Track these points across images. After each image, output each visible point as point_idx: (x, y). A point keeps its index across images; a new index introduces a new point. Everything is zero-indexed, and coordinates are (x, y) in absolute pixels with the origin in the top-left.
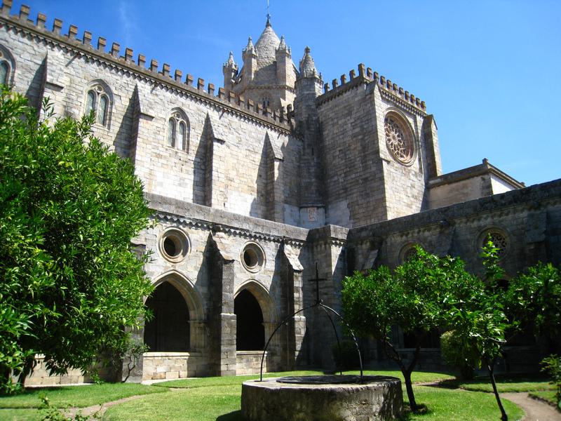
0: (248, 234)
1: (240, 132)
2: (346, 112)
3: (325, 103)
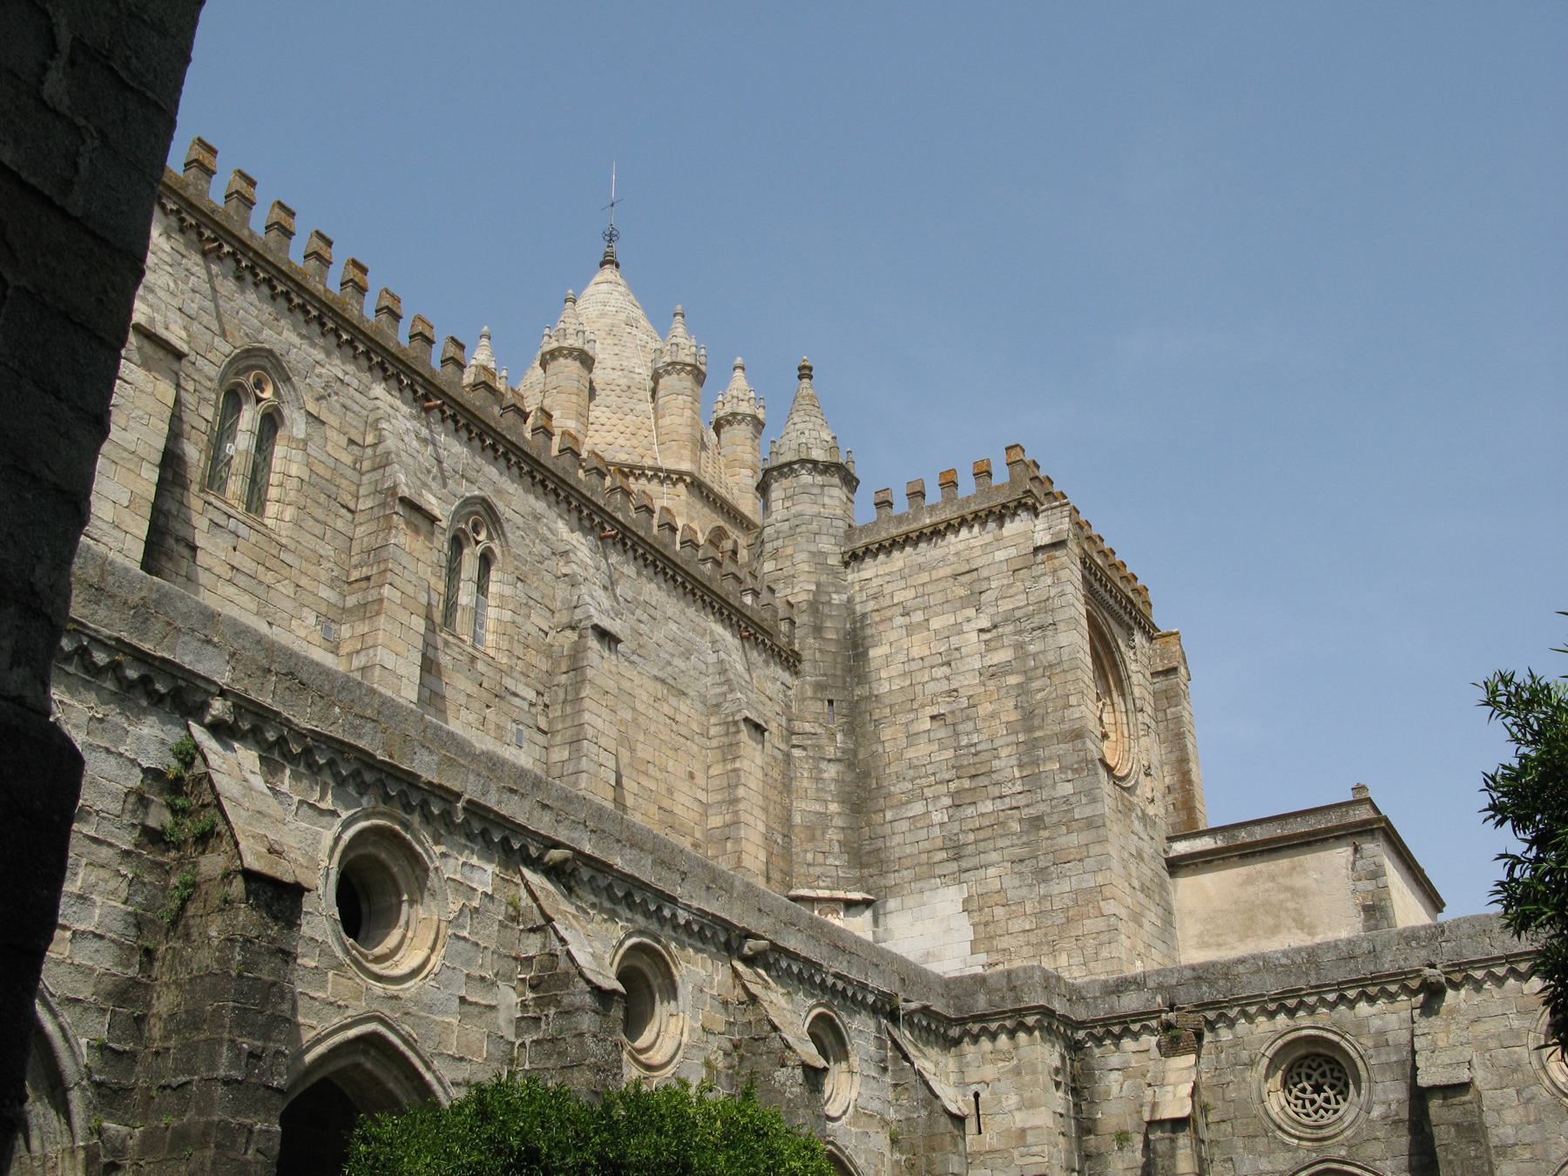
2: (962, 592)
3: (876, 556)
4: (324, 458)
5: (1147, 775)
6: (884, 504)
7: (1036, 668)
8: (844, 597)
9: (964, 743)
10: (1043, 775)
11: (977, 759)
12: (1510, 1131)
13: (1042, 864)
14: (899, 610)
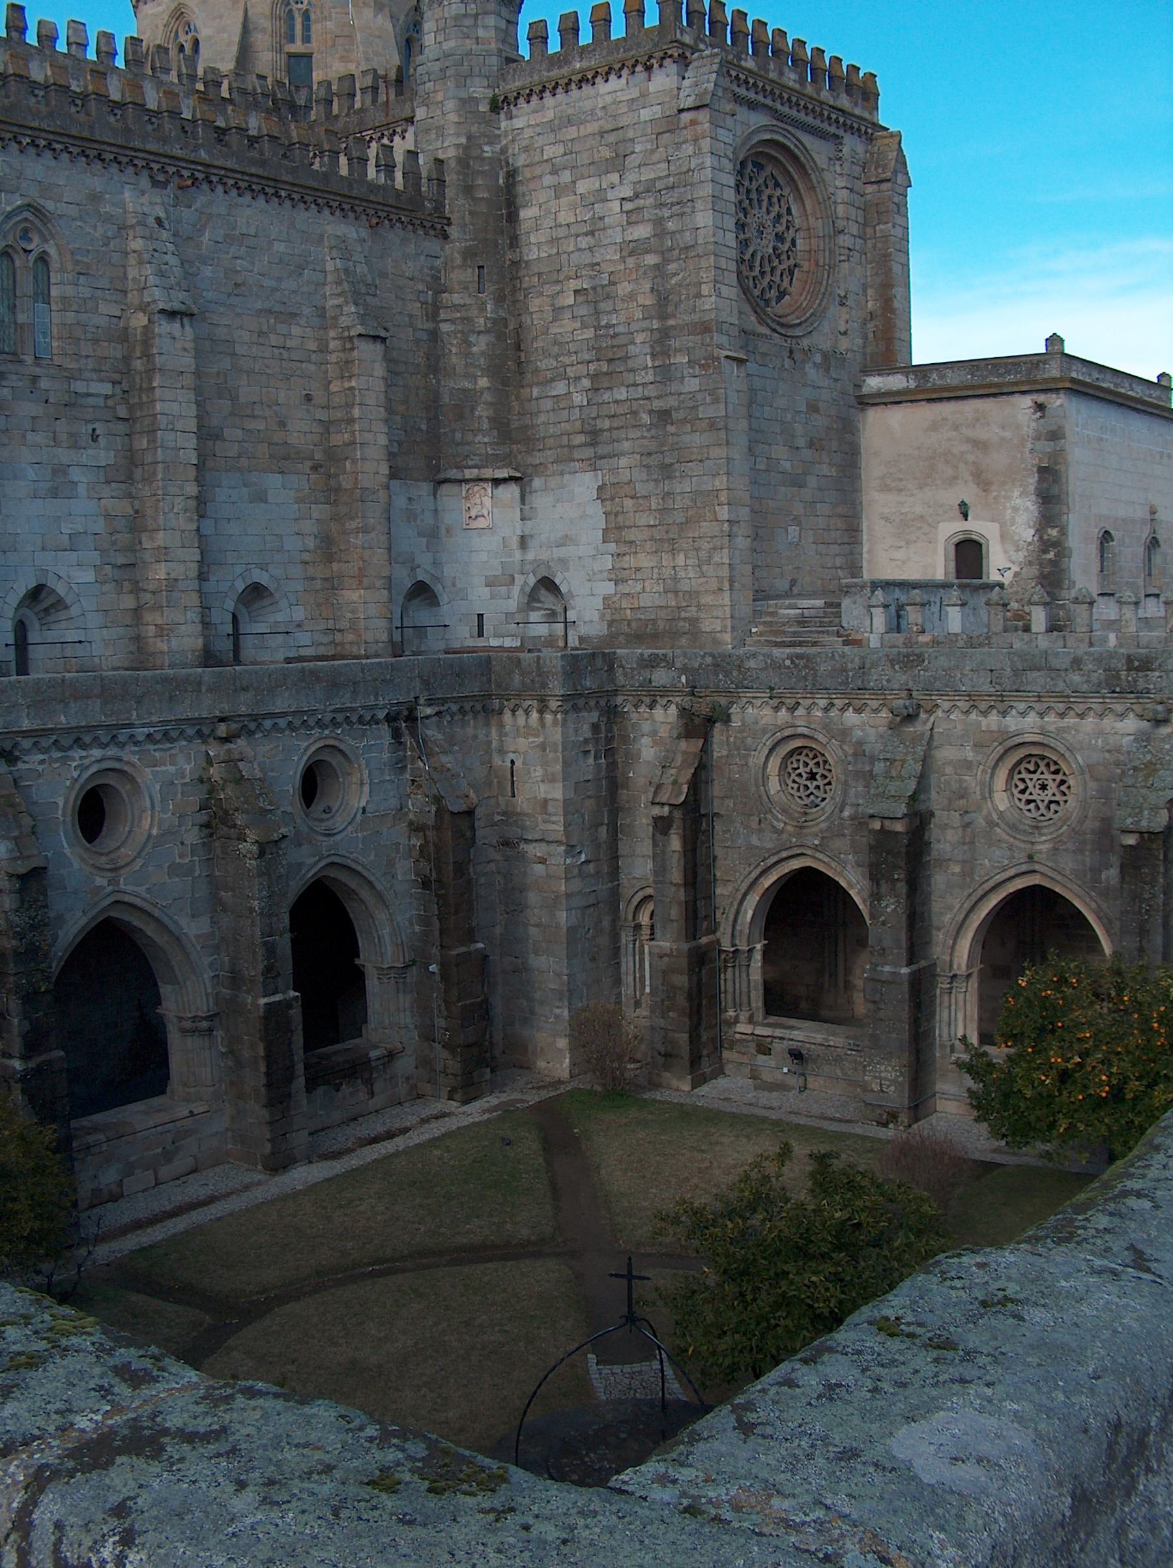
2: (606, 153)
5: (842, 304)
6: (538, 36)
7: (672, 249)
8: (498, 148)
9: (603, 323)
10: (673, 368)
11: (615, 342)
12: (948, 848)
13: (668, 461)
14: (548, 167)
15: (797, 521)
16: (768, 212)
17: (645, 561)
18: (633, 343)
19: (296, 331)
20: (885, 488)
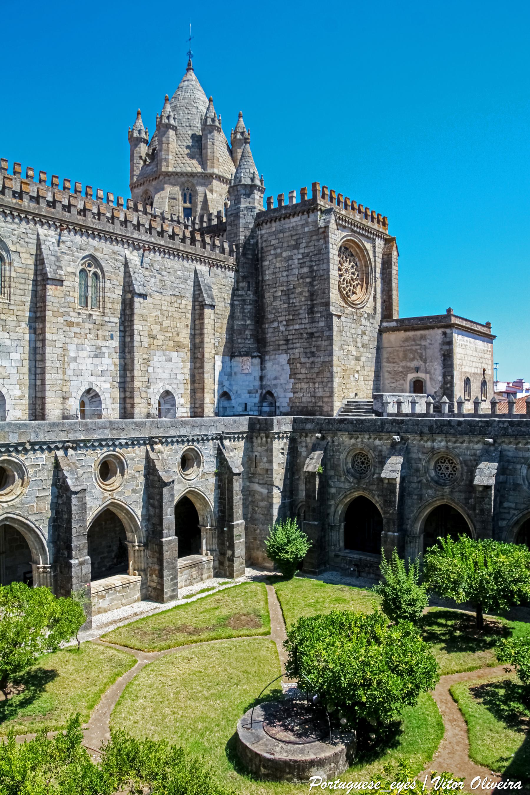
0: (185, 439)
1: (164, 273)
2: (293, 243)
3: (266, 224)
4: (21, 265)
7: (315, 277)
8: (255, 240)
11: (296, 309)
14: (273, 248)
15: (358, 372)
16: (349, 264)
17: (304, 386)
18: (301, 309)
19: (183, 302)
20: (389, 362)
